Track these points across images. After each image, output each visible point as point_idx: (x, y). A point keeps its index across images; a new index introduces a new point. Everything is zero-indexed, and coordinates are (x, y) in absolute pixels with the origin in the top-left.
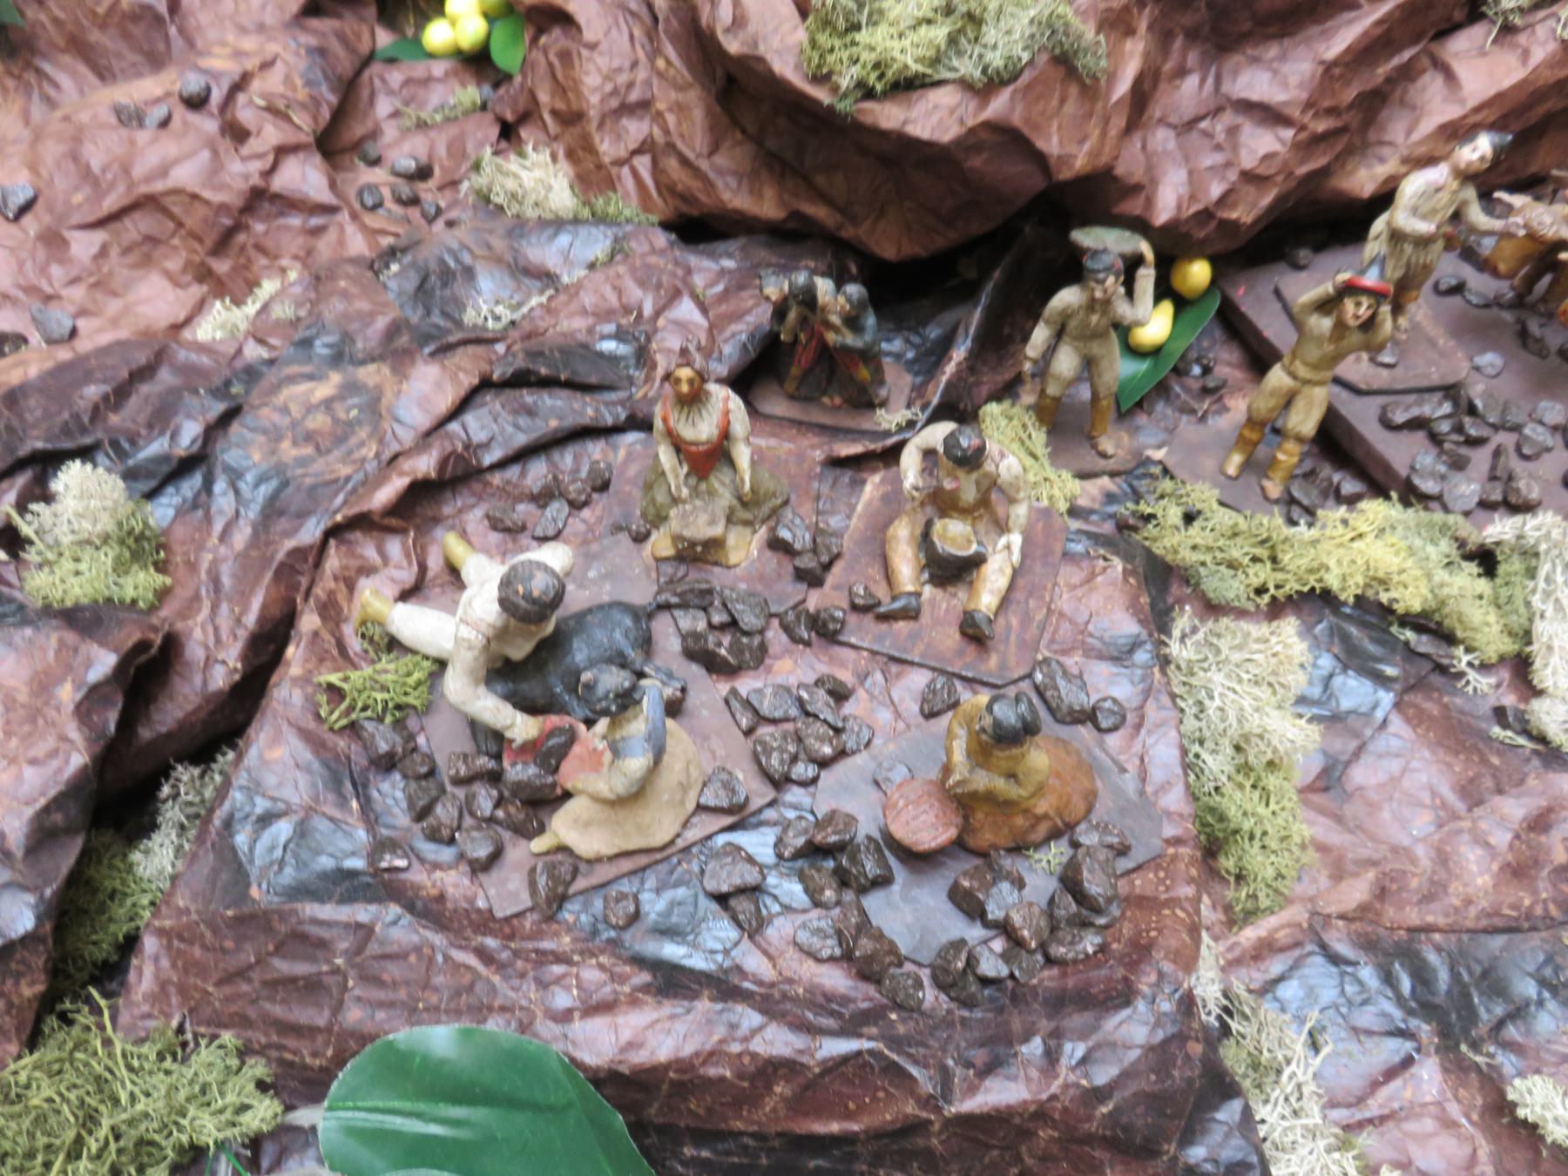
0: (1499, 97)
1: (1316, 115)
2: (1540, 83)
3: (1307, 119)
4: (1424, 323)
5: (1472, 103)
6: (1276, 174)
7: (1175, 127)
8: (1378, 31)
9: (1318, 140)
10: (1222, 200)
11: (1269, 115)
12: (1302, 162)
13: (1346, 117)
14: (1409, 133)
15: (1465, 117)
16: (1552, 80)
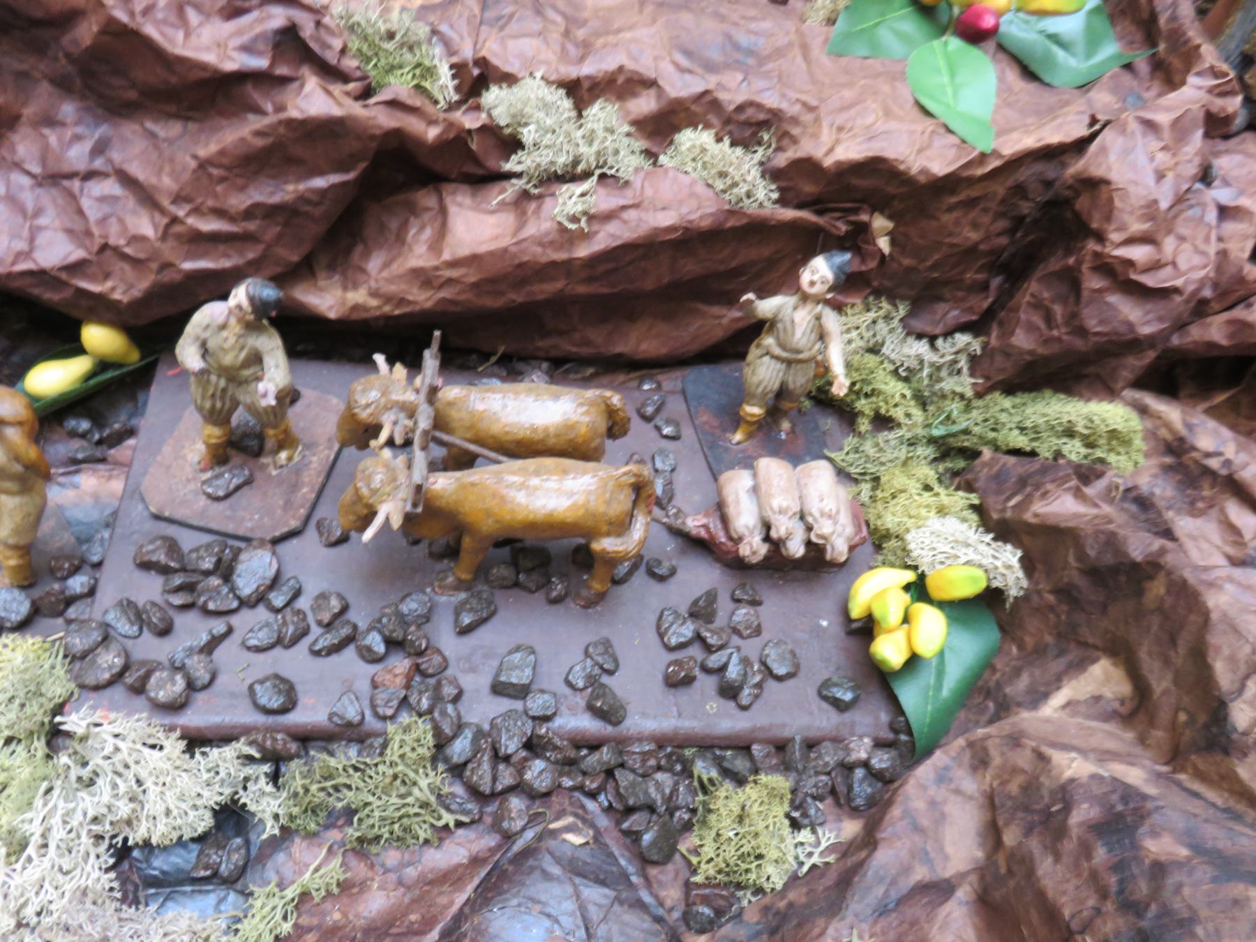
0: (473, 260)
1: (196, 211)
2: (526, 258)
3: (181, 213)
4: (314, 465)
5: (447, 256)
6: (148, 260)
7: (33, 176)
8: (260, 142)
9: (199, 242)
10: (76, 268)
11: (146, 196)
12: (190, 256)
13: (252, 226)
14: (386, 265)
15: (436, 268)
16: (544, 260)
